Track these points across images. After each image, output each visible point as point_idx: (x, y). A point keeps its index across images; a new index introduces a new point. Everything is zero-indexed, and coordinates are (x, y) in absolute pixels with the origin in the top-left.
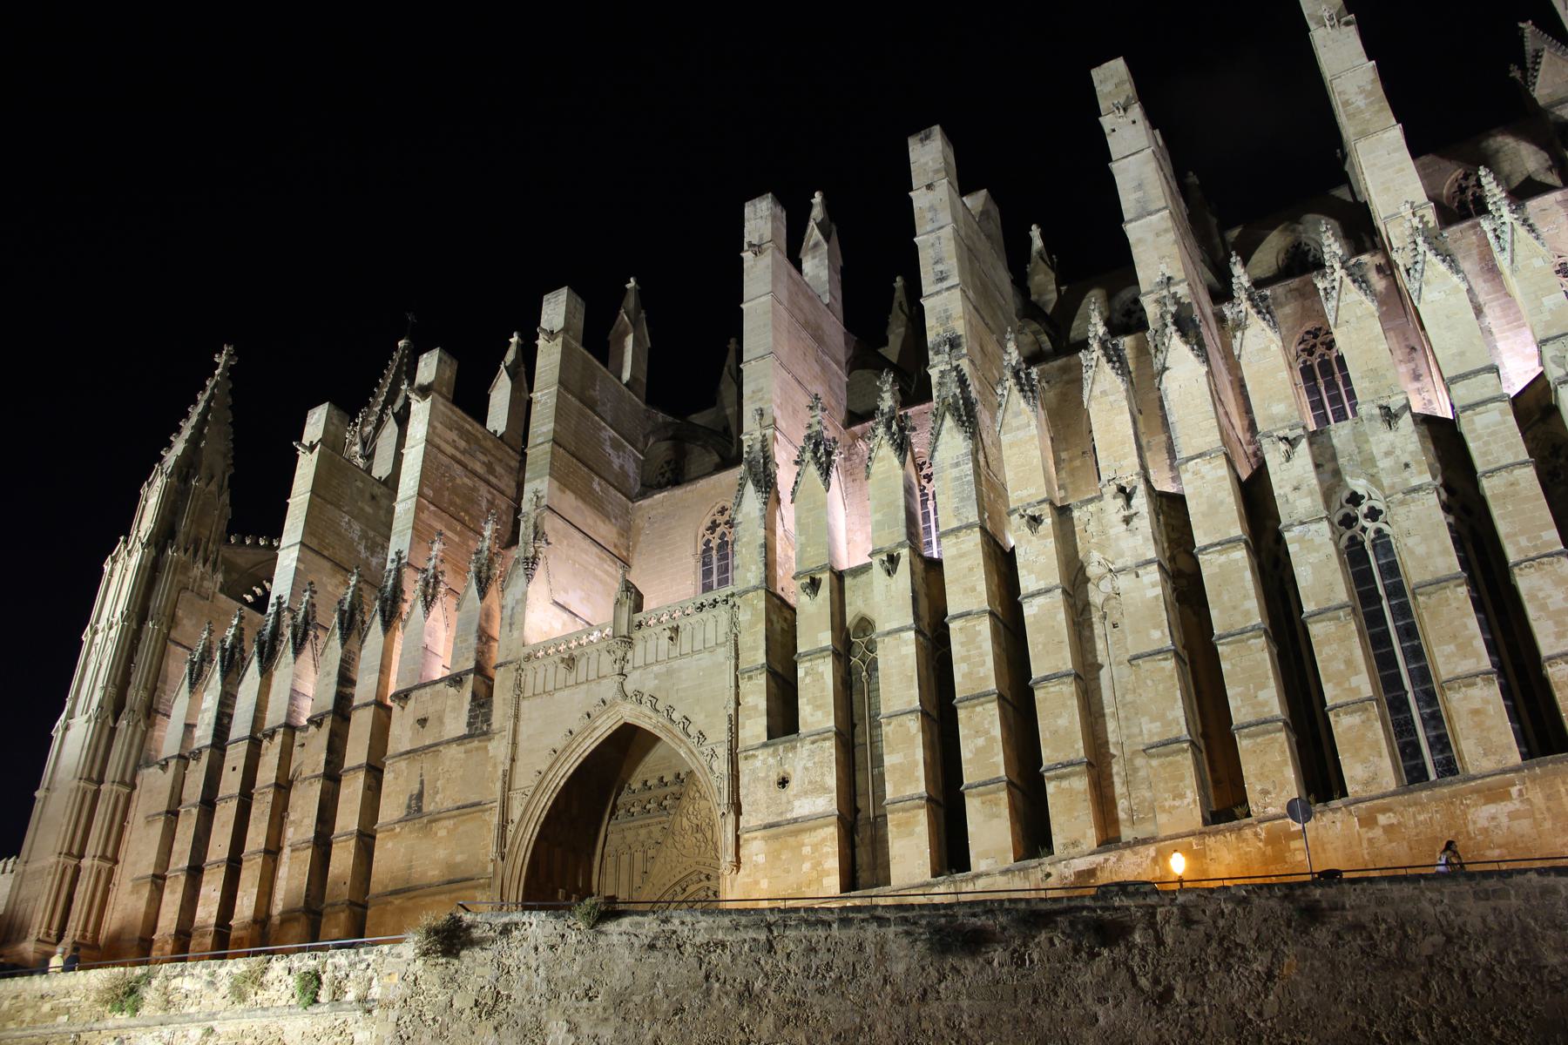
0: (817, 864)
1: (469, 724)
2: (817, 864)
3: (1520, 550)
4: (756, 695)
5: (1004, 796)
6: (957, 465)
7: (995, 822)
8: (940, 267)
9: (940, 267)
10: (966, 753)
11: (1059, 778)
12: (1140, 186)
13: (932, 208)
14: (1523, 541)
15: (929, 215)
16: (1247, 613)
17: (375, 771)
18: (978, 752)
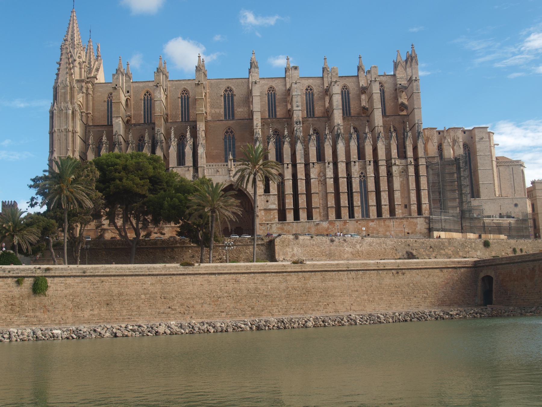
1: (193, 178)
2: (274, 216)
3: (382, 189)
5: (306, 210)
6: (301, 150)
7: (304, 214)
8: (297, 104)
9: (297, 104)
10: (300, 202)
11: (315, 209)
12: (337, 101)
13: (296, 88)
14: (383, 188)
15: (296, 90)
16: (345, 189)
18: (302, 202)
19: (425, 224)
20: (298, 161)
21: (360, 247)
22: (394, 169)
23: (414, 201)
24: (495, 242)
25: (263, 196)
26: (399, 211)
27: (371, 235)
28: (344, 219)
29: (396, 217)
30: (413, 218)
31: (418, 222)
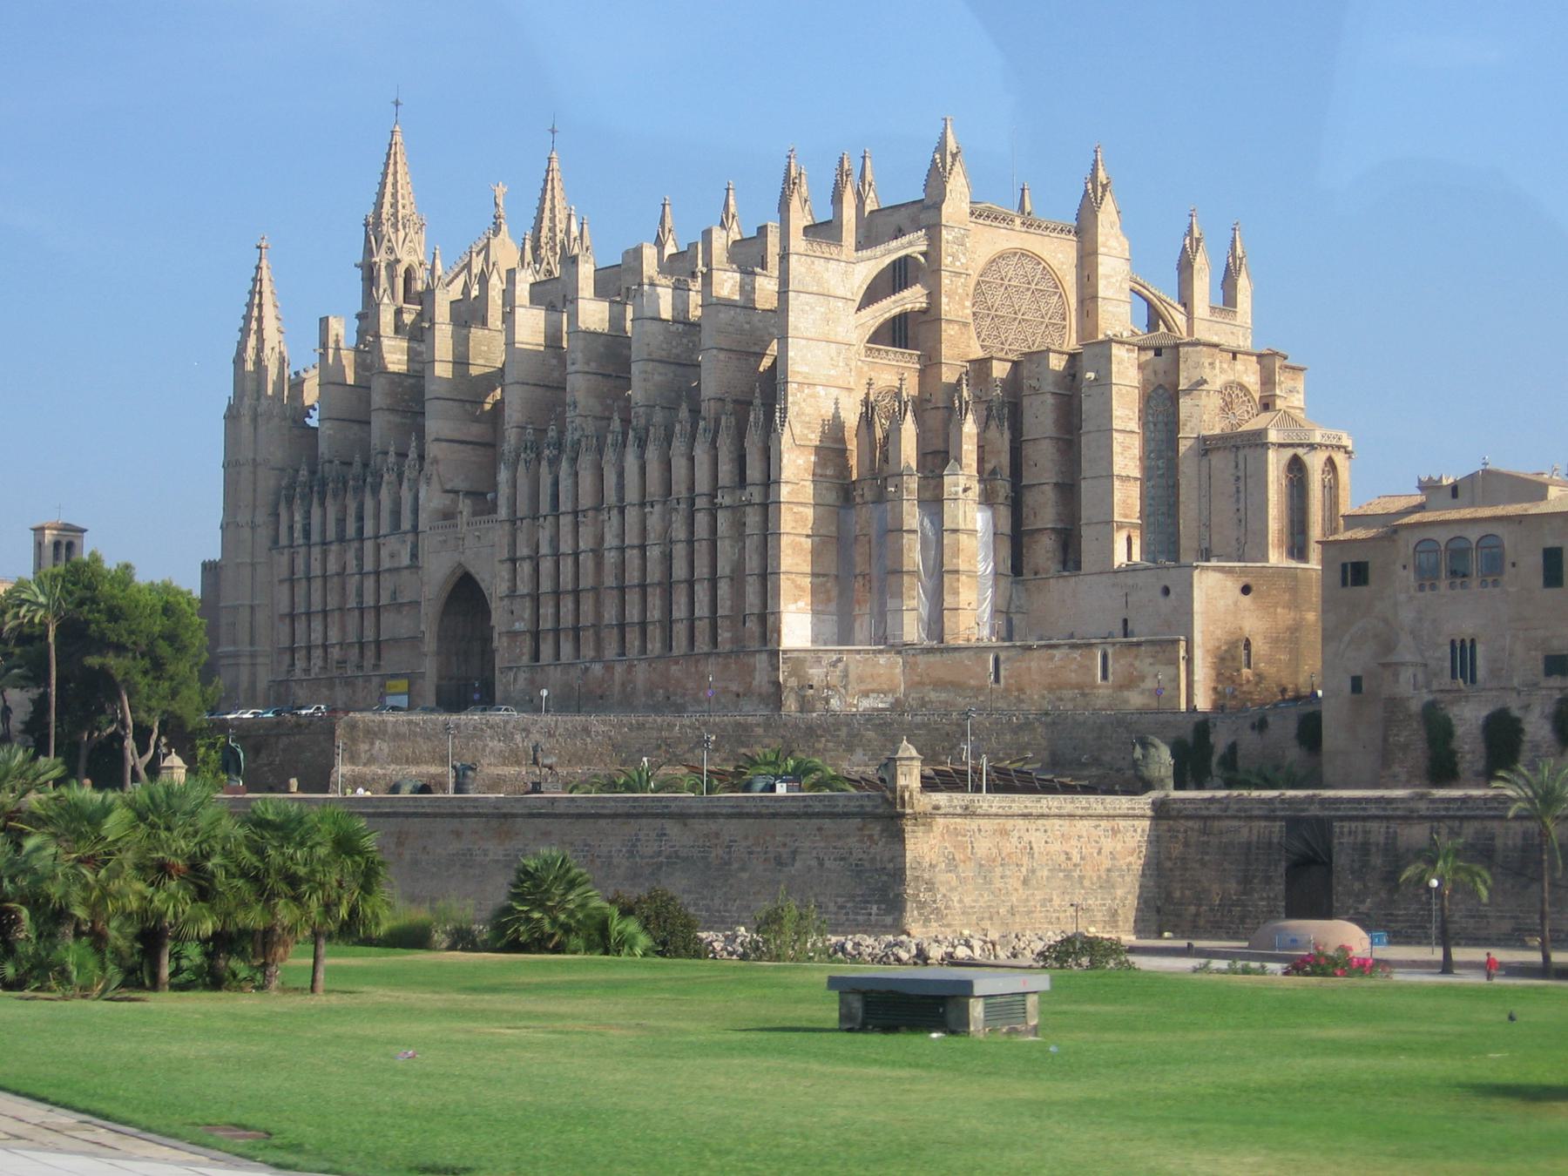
0: (521, 650)
1: (411, 560)
2: (521, 650)
4: (504, 571)
5: (571, 633)
17: (377, 573)
19: (770, 669)
20: (562, 508)
21: (523, 741)
22: (722, 517)
23: (751, 605)
24: (917, 725)
25: (506, 599)
26: (724, 635)
27: (672, 698)
28: (631, 656)
29: (718, 651)
30: (747, 653)
31: (757, 665)
